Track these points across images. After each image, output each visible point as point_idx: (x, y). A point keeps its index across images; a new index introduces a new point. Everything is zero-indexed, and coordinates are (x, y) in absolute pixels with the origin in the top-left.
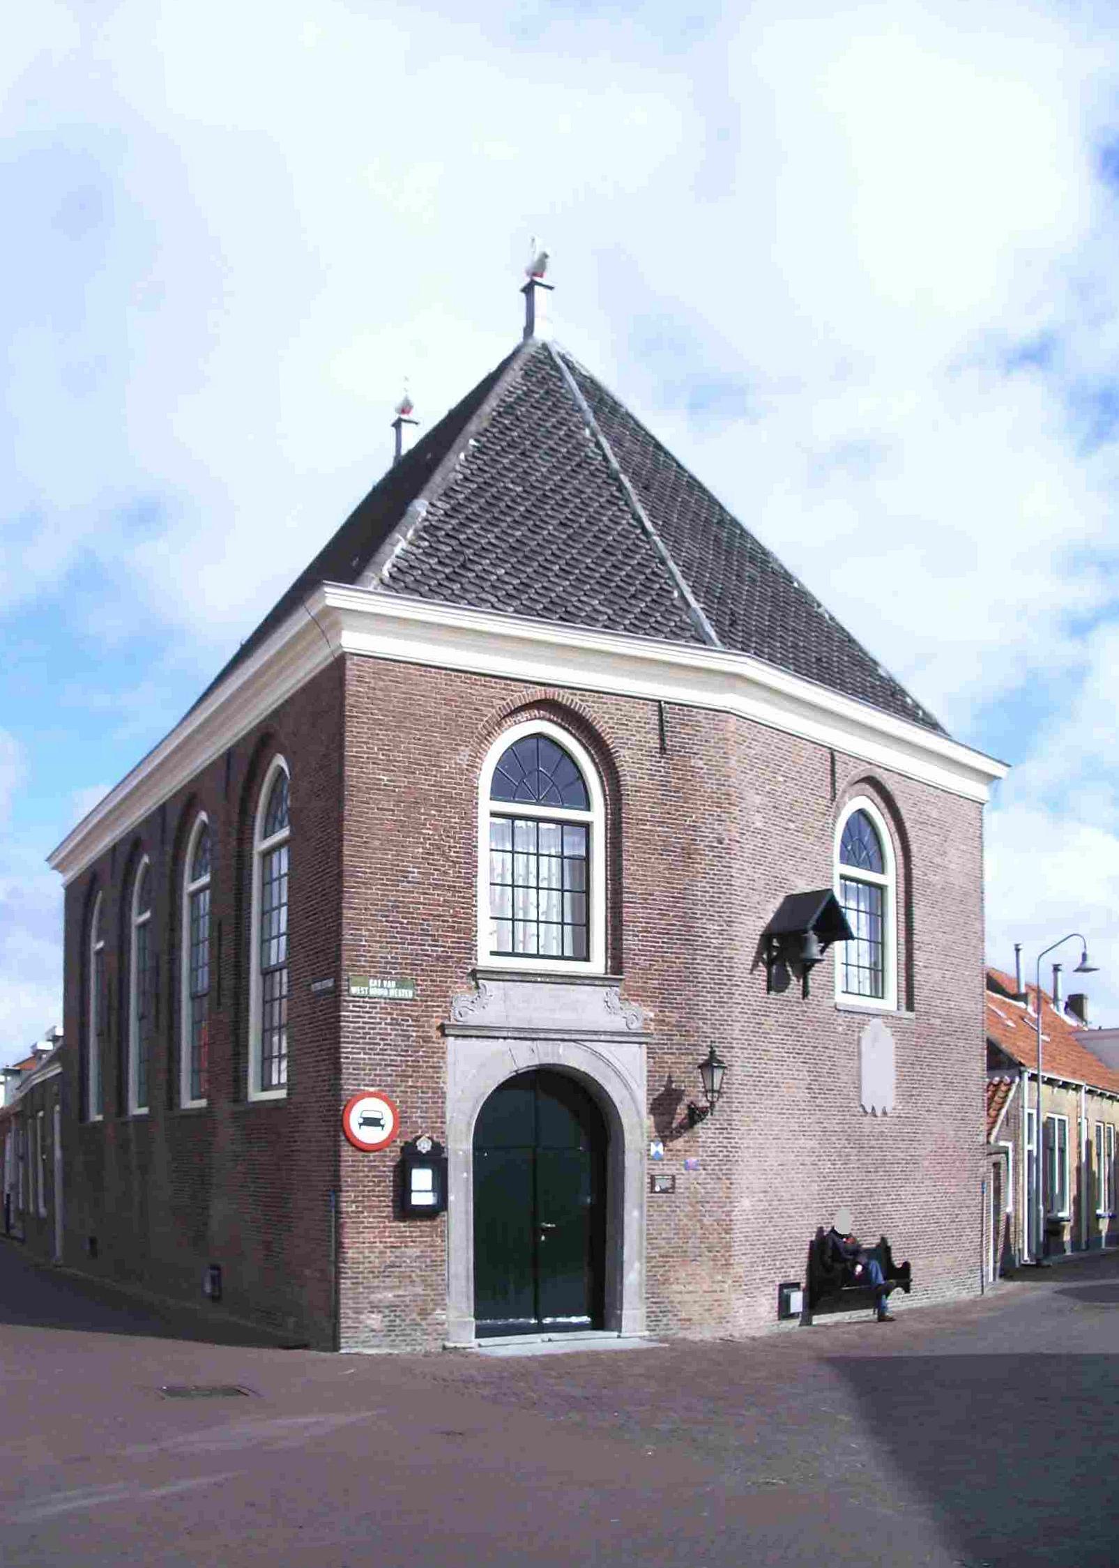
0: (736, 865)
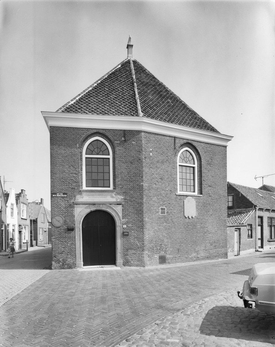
0: (144, 164)
